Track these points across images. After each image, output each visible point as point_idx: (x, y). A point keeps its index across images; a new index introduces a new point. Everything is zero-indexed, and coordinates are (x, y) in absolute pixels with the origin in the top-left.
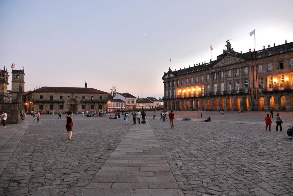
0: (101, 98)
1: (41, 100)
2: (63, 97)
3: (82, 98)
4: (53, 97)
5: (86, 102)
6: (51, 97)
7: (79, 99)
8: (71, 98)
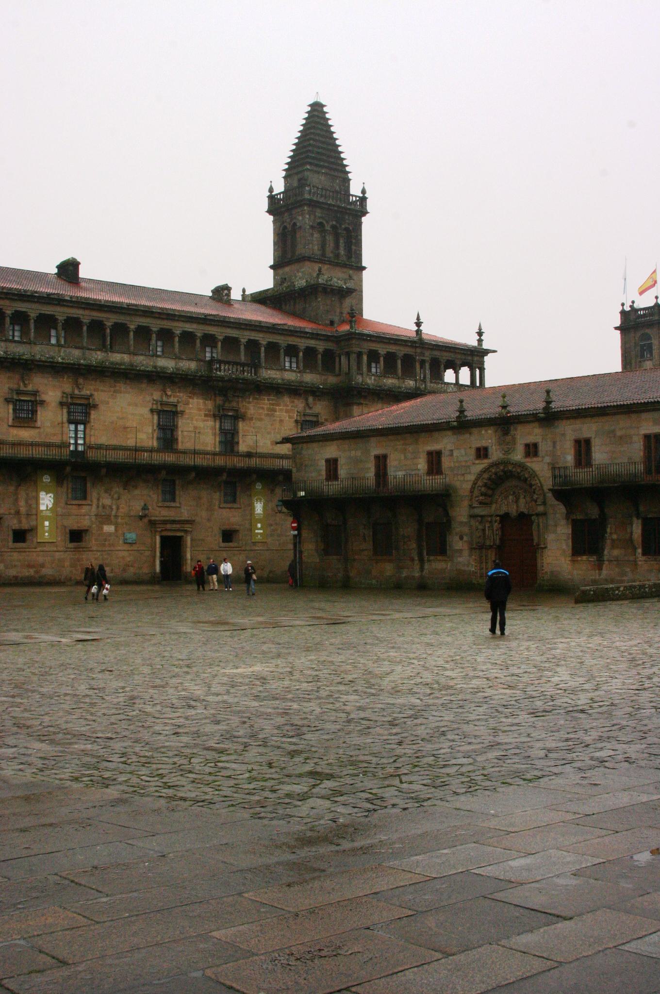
1: (333, 488)
2: (446, 463)
3: (570, 459)
6: (381, 461)
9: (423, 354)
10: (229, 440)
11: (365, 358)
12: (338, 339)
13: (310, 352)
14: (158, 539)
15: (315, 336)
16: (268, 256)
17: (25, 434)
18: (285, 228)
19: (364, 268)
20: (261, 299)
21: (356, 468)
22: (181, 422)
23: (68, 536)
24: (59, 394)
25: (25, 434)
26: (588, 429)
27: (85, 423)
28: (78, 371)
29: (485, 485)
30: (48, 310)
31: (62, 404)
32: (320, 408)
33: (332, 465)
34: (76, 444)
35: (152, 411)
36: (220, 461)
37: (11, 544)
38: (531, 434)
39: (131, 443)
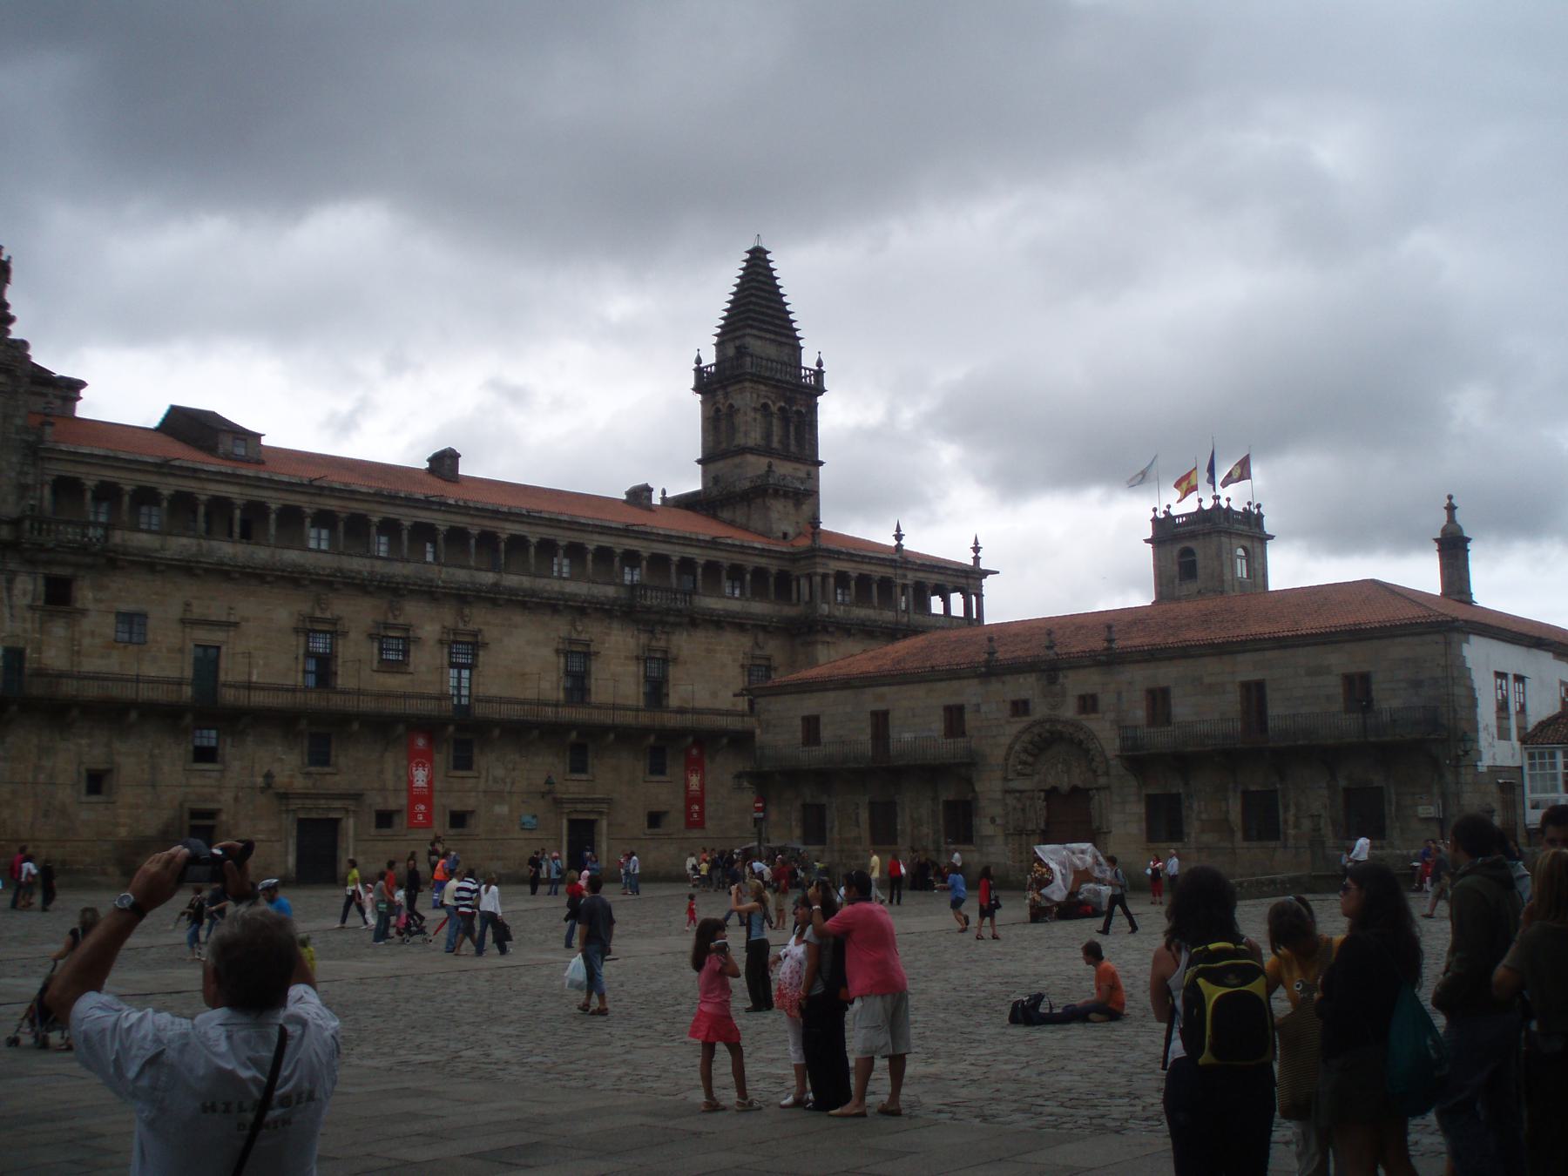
0: (1358, 688)
1: (811, 757)
3: (1140, 714)
4: (823, 720)
5: (1183, 762)
6: (880, 720)
7: (1104, 732)
8: (1040, 723)
9: (905, 576)
10: (656, 691)
11: (832, 581)
12: (794, 558)
13: (759, 573)
14: (565, 822)
15: (763, 552)
16: (693, 444)
17: (394, 682)
18: (718, 410)
19: (821, 463)
20: (687, 503)
21: (846, 726)
22: (595, 667)
23: (448, 818)
24: (438, 627)
25: (394, 682)
26: (1165, 674)
27: (470, 667)
28: (463, 597)
29: (1025, 751)
30: (425, 516)
31: (441, 642)
32: (773, 648)
33: (811, 726)
34: (460, 696)
35: (557, 651)
36: (645, 719)
37: (373, 831)
38: (1089, 681)
39: (530, 694)
